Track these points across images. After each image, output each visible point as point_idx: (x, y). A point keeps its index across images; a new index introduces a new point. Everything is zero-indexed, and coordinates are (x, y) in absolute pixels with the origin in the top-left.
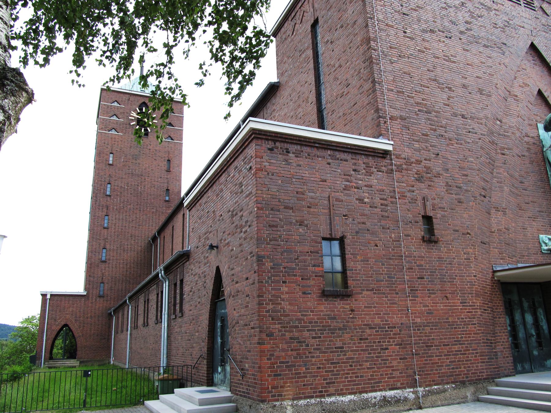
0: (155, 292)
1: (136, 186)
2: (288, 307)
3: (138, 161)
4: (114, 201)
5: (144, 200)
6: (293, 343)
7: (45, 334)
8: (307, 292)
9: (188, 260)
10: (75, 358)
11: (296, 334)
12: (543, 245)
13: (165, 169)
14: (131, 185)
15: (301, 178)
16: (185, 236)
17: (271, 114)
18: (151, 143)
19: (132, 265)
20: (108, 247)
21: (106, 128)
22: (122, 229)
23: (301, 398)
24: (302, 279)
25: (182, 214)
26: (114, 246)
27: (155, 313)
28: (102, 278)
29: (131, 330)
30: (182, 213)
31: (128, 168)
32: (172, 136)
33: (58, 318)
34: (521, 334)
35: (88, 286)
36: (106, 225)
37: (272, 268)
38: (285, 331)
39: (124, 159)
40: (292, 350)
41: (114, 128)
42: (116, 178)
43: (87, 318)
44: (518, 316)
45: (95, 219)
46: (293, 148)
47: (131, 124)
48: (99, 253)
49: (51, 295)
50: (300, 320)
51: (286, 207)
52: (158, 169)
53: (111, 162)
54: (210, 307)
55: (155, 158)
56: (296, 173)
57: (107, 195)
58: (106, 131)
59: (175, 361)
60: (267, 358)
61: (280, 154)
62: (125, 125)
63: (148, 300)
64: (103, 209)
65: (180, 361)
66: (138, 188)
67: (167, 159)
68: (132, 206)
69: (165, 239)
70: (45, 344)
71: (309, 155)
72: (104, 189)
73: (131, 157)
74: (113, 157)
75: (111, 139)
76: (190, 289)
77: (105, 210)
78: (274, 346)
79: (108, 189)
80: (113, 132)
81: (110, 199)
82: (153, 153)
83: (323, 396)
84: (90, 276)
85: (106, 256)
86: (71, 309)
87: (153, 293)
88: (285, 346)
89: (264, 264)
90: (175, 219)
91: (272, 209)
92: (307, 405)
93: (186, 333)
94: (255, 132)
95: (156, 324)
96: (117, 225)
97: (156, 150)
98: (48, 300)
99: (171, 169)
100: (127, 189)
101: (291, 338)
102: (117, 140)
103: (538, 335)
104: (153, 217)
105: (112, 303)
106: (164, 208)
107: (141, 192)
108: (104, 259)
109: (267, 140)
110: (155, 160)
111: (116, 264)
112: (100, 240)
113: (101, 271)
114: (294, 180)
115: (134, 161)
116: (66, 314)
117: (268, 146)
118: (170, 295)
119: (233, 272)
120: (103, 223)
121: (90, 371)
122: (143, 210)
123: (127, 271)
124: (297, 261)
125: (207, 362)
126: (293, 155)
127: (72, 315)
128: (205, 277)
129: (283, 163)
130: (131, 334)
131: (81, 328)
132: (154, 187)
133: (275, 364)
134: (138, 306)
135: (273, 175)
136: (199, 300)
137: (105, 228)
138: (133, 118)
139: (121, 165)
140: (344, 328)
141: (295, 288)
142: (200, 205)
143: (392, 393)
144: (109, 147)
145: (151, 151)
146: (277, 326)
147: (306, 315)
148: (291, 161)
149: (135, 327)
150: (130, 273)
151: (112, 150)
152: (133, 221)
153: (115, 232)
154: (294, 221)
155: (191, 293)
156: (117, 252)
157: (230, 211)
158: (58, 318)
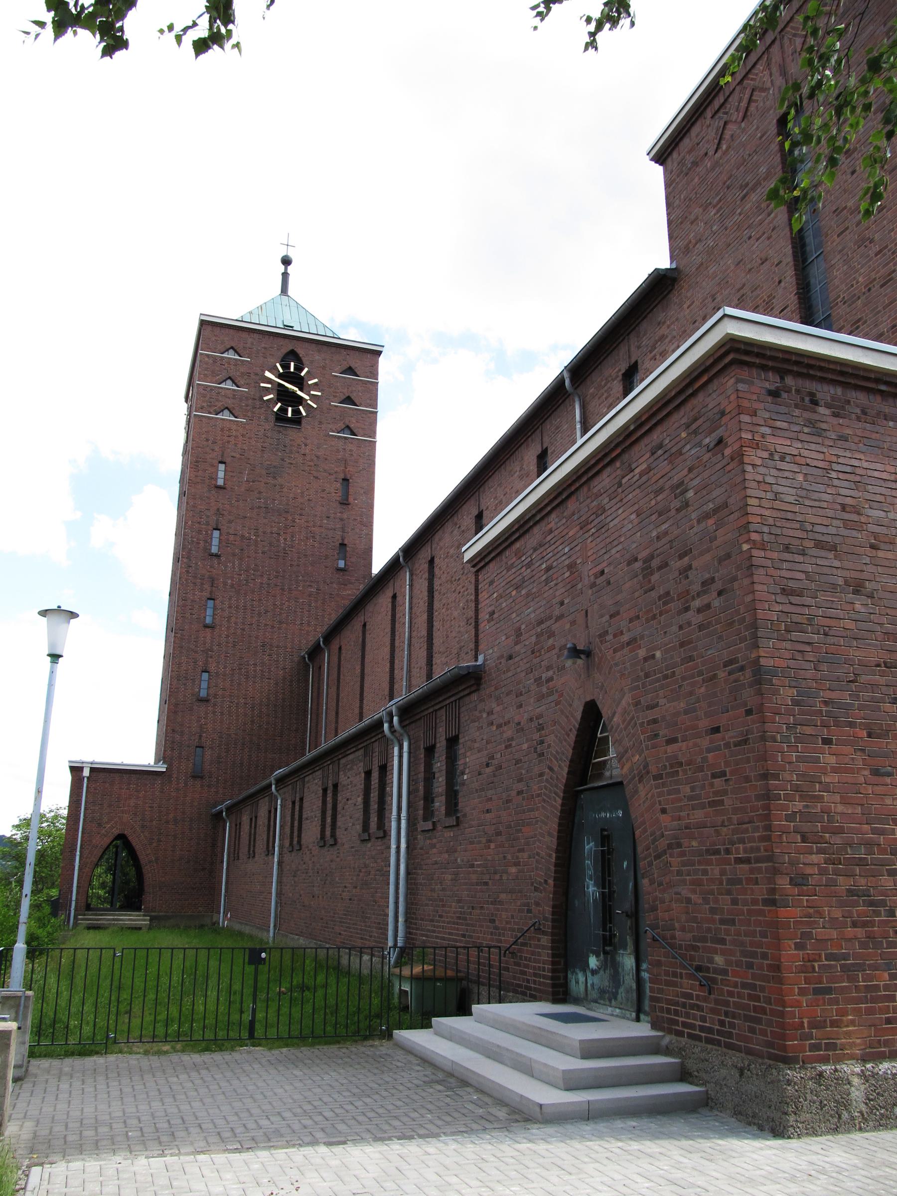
0: (361, 768)
1: (275, 535)
2: (840, 808)
3: (280, 480)
4: (226, 566)
5: (291, 565)
6: (855, 904)
7: (78, 853)
8: (883, 770)
9: (477, 690)
10: (139, 909)
13: (338, 499)
14: (264, 533)
15: (848, 469)
16: (397, 644)
17: (654, 347)
18: (308, 441)
19: (264, 710)
20: (212, 668)
21: (210, 406)
22: (243, 629)
24: (869, 736)
25: (391, 594)
26: (225, 667)
27: (360, 815)
28: (201, 736)
29: (280, 854)
30: (389, 593)
31: (258, 495)
32: (352, 426)
33: (105, 819)
35: (169, 752)
36: (208, 620)
37: (796, 703)
38: (837, 873)
39: (248, 475)
40: (854, 925)
41: (227, 408)
42: (232, 518)
43: (167, 822)
45: (185, 606)
46: (826, 392)
47: (265, 398)
48: (193, 680)
49: (92, 770)
51: (819, 545)
52: (323, 498)
53: (220, 482)
54: (563, 805)
55: (315, 474)
56: (838, 456)
57: (212, 555)
58: (210, 413)
59: (434, 932)
60: (796, 944)
61: (796, 406)
62: (250, 402)
63: (336, 786)
64: (202, 584)
65: (450, 934)
66: (278, 541)
67: (342, 476)
68: (265, 580)
69: (343, 651)
70: (79, 875)
71: (864, 413)
72: (206, 542)
73: (264, 472)
74: (225, 471)
75: (222, 430)
76: (484, 760)
77: (207, 586)
78: (811, 911)
79: (215, 542)
80: (226, 416)
81: (219, 563)
82: (312, 464)
84: (173, 731)
85: (208, 688)
86: (132, 802)
87: (351, 769)
88: (837, 913)
89: (776, 693)
90: (370, 607)
91: (787, 548)
93: (472, 866)
94: (737, 345)
95: (363, 841)
96: (233, 619)
97: (318, 457)
98: (86, 780)
99: (351, 500)
100: (256, 541)
101: (851, 892)
102: (234, 433)
104: (310, 605)
105: (221, 792)
106: (335, 585)
107: (284, 549)
108: (203, 693)
109: (764, 368)
110: (317, 478)
111: (230, 707)
112: (196, 652)
113: (198, 721)
114: (834, 475)
115: (271, 480)
116: (123, 812)
117: (767, 385)
118: (413, 773)
119: (651, 715)
120: (202, 615)
121: (264, 950)
122: (290, 589)
123: (253, 722)
124: (853, 685)
125: (553, 941)
126: (827, 412)
127: (135, 814)
128: (541, 728)
129: (806, 430)
130: (280, 863)
131: (154, 844)
132: (313, 537)
133: (815, 961)
134: (301, 799)
135: (782, 459)
136: (521, 786)
137: (206, 626)
138: (269, 386)
139: (243, 489)
141: (853, 759)
142: (519, 554)
144: (217, 449)
145: (308, 458)
146: (815, 858)
147: (882, 832)
148: (824, 426)
149: (295, 843)
150: (260, 726)
151: (222, 456)
152: (266, 612)
153: (227, 636)
154: (840, 582)
155: (488, 770)
156: (232, 681)
157: (636, 560)
158: (105, 819)
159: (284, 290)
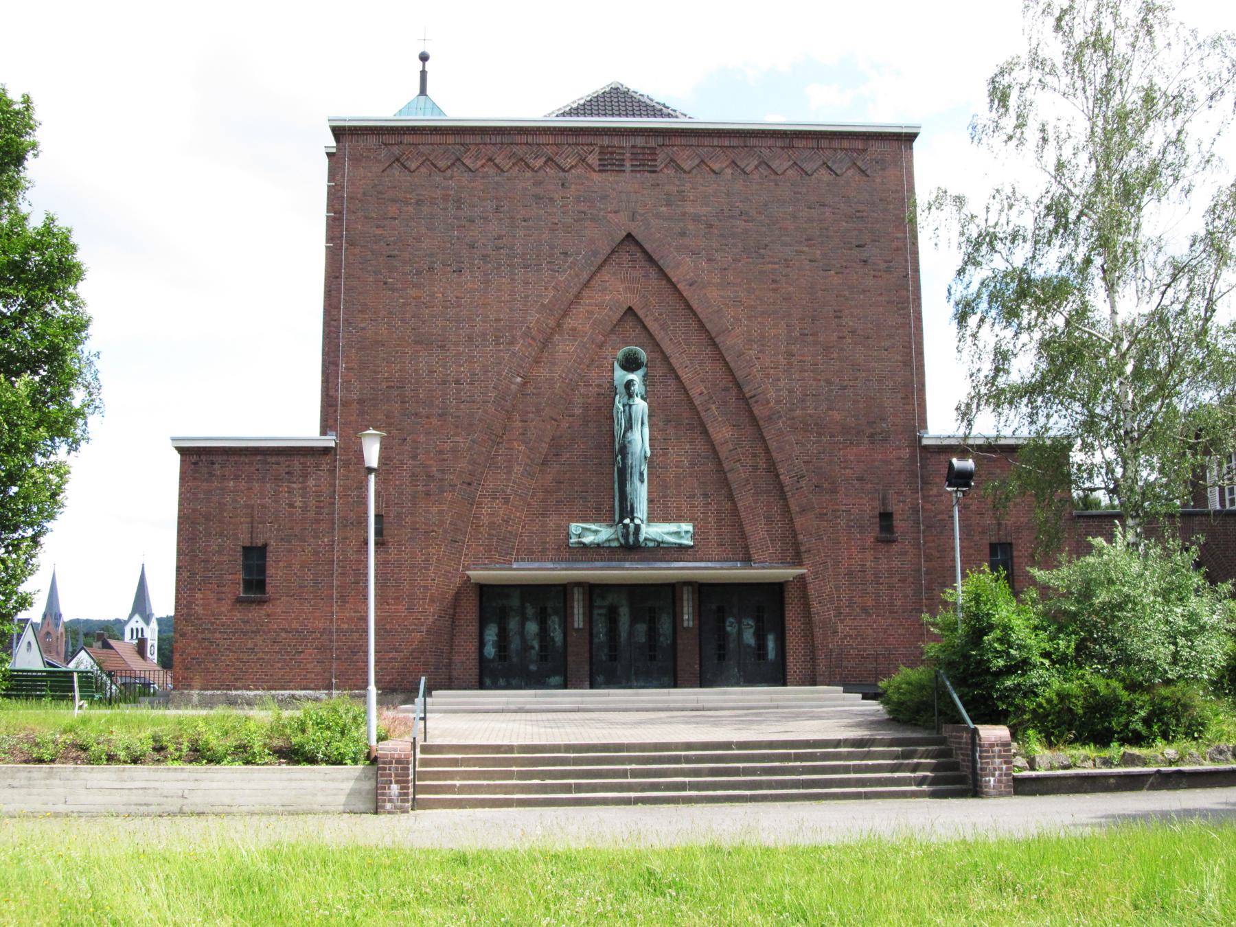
11: (209, 636)
23: (208, 689)
34: (515, 644)
44: (513, 624)
50: (212, 624)
83: (230, 690)
88: (197, 645)
92: (213, 695)
103: (543, 648)
140: (258, 631)
143: (302, 693)
159: (423, 91)
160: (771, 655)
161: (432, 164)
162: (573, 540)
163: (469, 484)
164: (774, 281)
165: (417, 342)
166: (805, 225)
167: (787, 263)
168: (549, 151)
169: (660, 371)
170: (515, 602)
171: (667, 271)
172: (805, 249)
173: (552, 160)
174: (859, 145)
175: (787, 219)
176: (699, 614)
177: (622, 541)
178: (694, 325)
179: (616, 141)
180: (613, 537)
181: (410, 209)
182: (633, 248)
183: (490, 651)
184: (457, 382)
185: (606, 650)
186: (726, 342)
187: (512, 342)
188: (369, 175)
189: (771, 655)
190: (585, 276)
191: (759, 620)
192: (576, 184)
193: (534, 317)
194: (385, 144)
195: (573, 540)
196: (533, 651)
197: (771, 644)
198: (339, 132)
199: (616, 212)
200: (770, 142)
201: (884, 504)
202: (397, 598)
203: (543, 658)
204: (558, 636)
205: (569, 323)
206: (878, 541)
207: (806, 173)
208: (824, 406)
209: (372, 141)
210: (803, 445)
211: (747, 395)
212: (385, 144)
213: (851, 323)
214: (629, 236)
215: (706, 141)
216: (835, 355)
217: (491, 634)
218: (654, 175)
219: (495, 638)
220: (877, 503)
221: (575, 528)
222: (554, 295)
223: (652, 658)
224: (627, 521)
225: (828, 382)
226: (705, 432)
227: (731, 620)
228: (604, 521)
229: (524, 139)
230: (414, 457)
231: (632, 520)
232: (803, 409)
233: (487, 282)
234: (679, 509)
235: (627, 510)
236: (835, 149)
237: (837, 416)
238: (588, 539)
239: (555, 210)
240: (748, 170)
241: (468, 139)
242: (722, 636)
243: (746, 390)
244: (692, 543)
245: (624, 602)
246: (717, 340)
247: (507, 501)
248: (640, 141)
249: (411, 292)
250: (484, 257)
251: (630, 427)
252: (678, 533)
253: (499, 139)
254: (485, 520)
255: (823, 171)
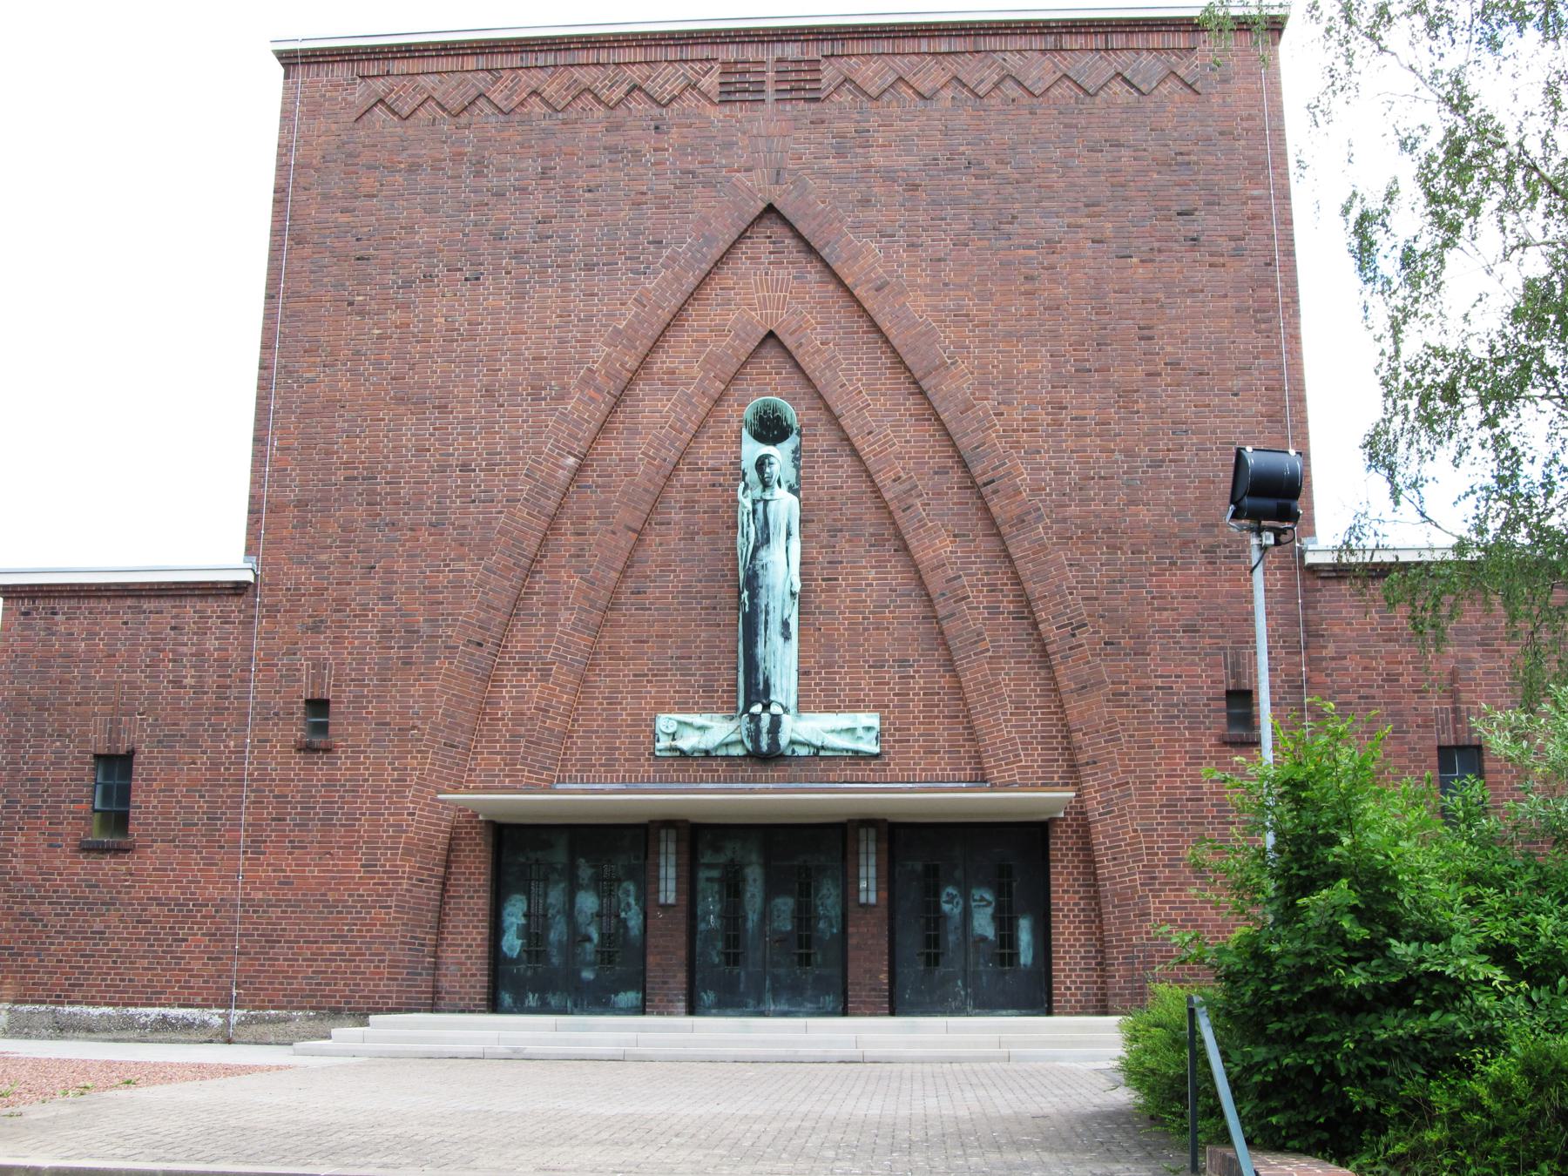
6: (24, 920)
11: (33, 908)
12: (662, 737)
23: (26, 1002)
34: (557, 933)
38: (14, 903)
40: (20, 931)
83: (61, 1003)
88: (11, 925)
92: (31, 1013)
101: (22, 914)
143: (181, 1012)
147: (49, 880)
160: (1026, 956)
161: (438, 104)
162: (664, 743)
163: (480, 645)
164: (1028, 278)
165: (401, 400)
166: (1083, 181)
167: (1051, 245)
168: (635, 74)
169: (824, 439)
170: (560, 857)
171: (836, 266)
172: (1084, 221)
173: (640, 89)
174: (1181, 40)
175: (1051, 171)
176: (890, 879)
177: (749, 745)
178: (886, 360)
179: (750, 52)
180: (734, 737)
181: (399, 178)
182: (778, 230)
183: (512, 943)
184: (465, 467)
185: (720, 945)
186: (943, 388)
187: (562, 397)
188: (334, 127)
189: (1026, 956)
190: (691, 280)
191: (1002, 891)
192: (679, 126)
193: (600, 351)
194: (363, 77)
195: (664, 743)
196: (589, 947)
197: (1025, 937)
198: (290, 60)
199: (746, 170)
200: (1020, 42)
201: (1236, 675)
202: (348, 847)
203: (606, 957)
204: (634, 921)
205: (662, 362)
206: (1226, 743)
207: (1086, 92)
208: (1121, 496)
209: (341, 72)
210: (1082, 568)
211: (979, 481)
212: (363, 77)
213: (1169, 349)
214: (770, 209)
215: (909, 45)
216: (1141, 406)
217: (515, 913)
218: (813, 106)
219: (523, 921)
220: (1222, 673)
221: (666, 722)
222: (637, 315)
223: (805, 960)
224: (757, 708)
225: (1129, 453)
226: (904, 548)
227: (951, 890)
228: (720, 709)
229: (592, 56)
230: (387, 598)
231: (766, 707)
232: (1084, 502)
233: (521, 296)
234: (855, 687)
235: (758, 691)
236: (1138, 50)
237: (1145, 515)
238: (688, 742)
239: (642, 171)
240: (982, 90)
241: (499, 61)
242: (934, 919)
243: (977, 469)
244: (876, 750)
245: (754, 857)
246: (925, 384)
247: (545, 674)
248: (792, 51)
249: (395, 317)
250: (518, 254)
251: (764, 540)
252: (851, 730)
253: (550, 59)
254: (507, 708)
255: (1117, 87)
